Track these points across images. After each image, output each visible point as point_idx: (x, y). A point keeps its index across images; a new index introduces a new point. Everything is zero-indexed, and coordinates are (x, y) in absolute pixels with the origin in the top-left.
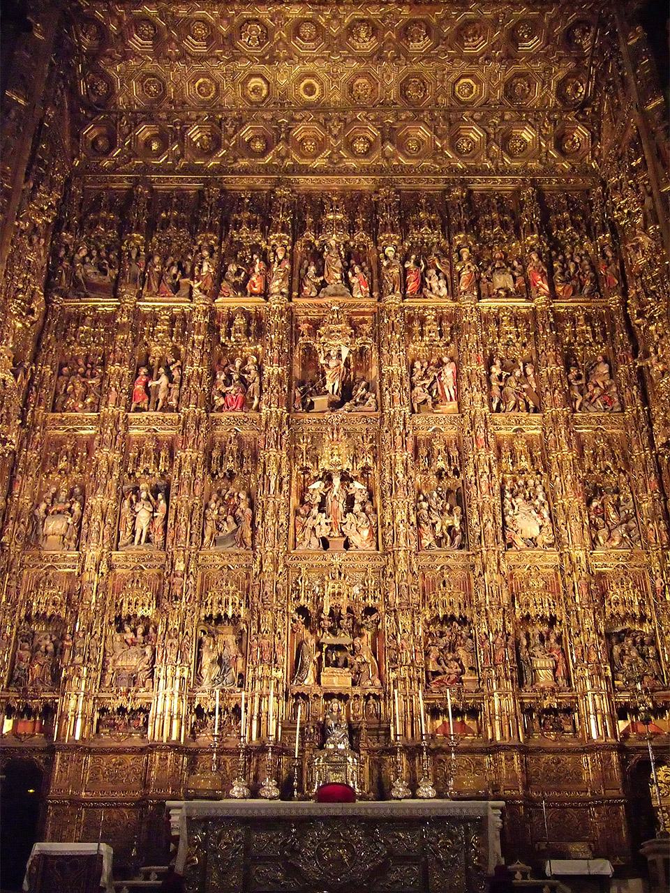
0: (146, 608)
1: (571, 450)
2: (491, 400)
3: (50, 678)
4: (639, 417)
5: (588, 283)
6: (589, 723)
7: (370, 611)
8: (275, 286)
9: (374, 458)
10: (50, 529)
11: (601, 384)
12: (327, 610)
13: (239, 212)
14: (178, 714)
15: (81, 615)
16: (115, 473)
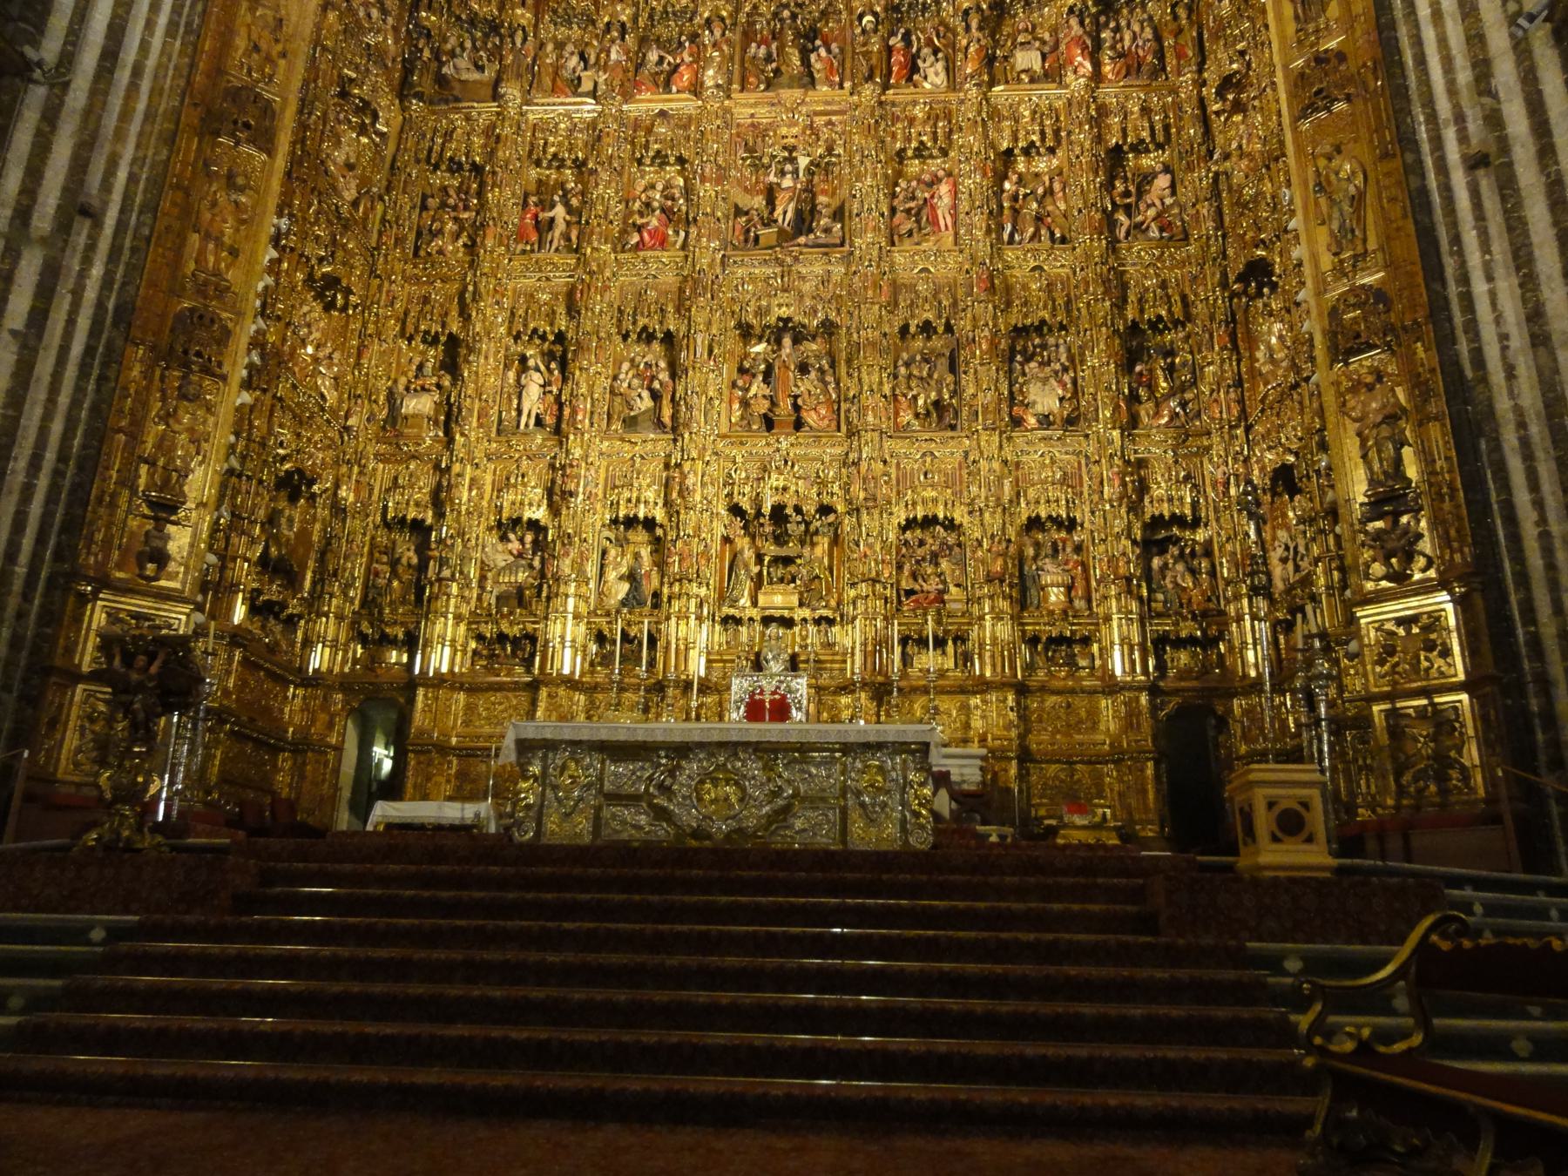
7: (825, 510)
8: (710, 76)
11: (1158, 203)
12: (767, 509)
14: (573, 641)
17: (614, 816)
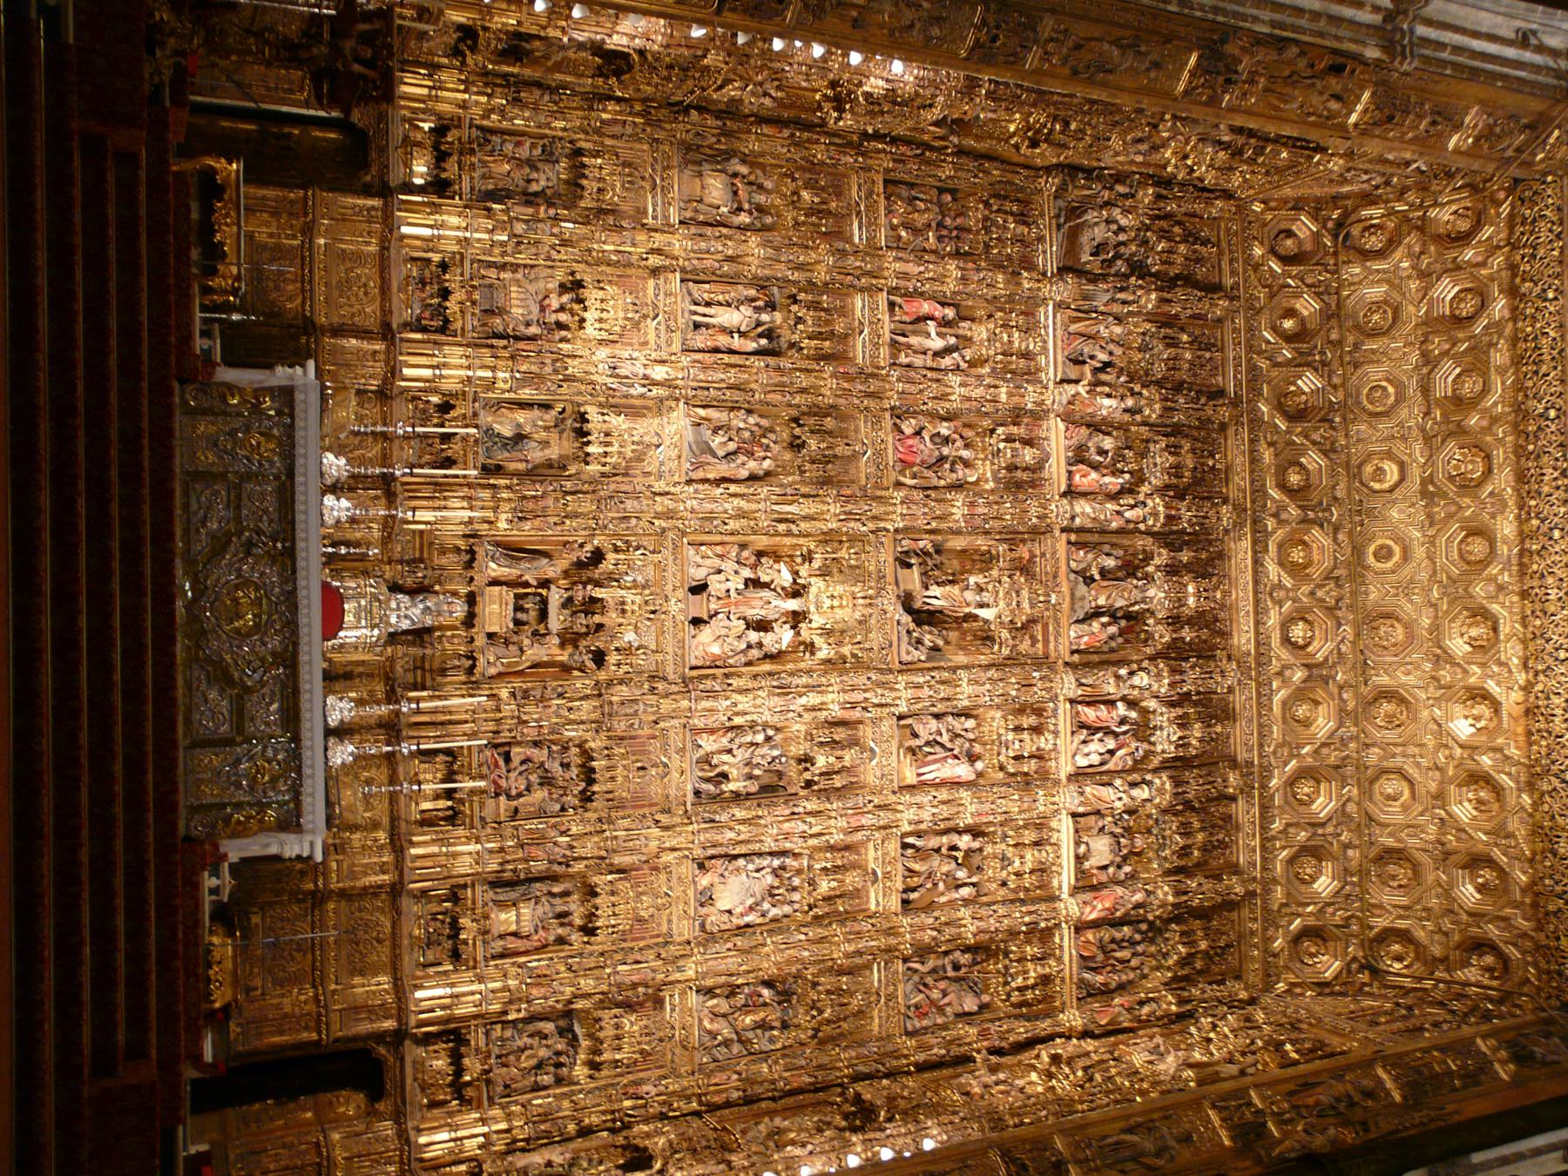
0: (597, 325)
1: (847, 955)
2: (919, 834)
3: (491, 187)
4: (897, 1058)
5: (1100, 979)
6: (438, 986)
7: (599, 658)
8: (1084, 507)
9: (829, 661)
11: (946, 1000)
12: (599, 593)
13: (1193, 450)
14: (441, 376)
15: (584, 230)
17: (215, 493)
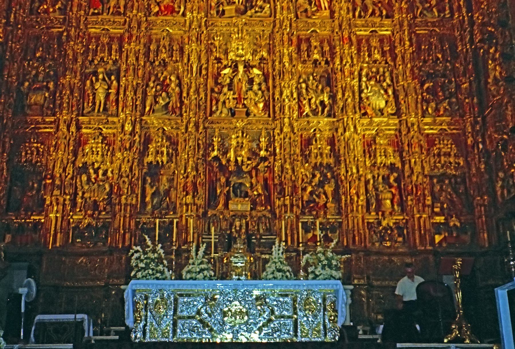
1: (411, 45)
2: (354, 10)
10: (32, 100)
16: (79, 60)
